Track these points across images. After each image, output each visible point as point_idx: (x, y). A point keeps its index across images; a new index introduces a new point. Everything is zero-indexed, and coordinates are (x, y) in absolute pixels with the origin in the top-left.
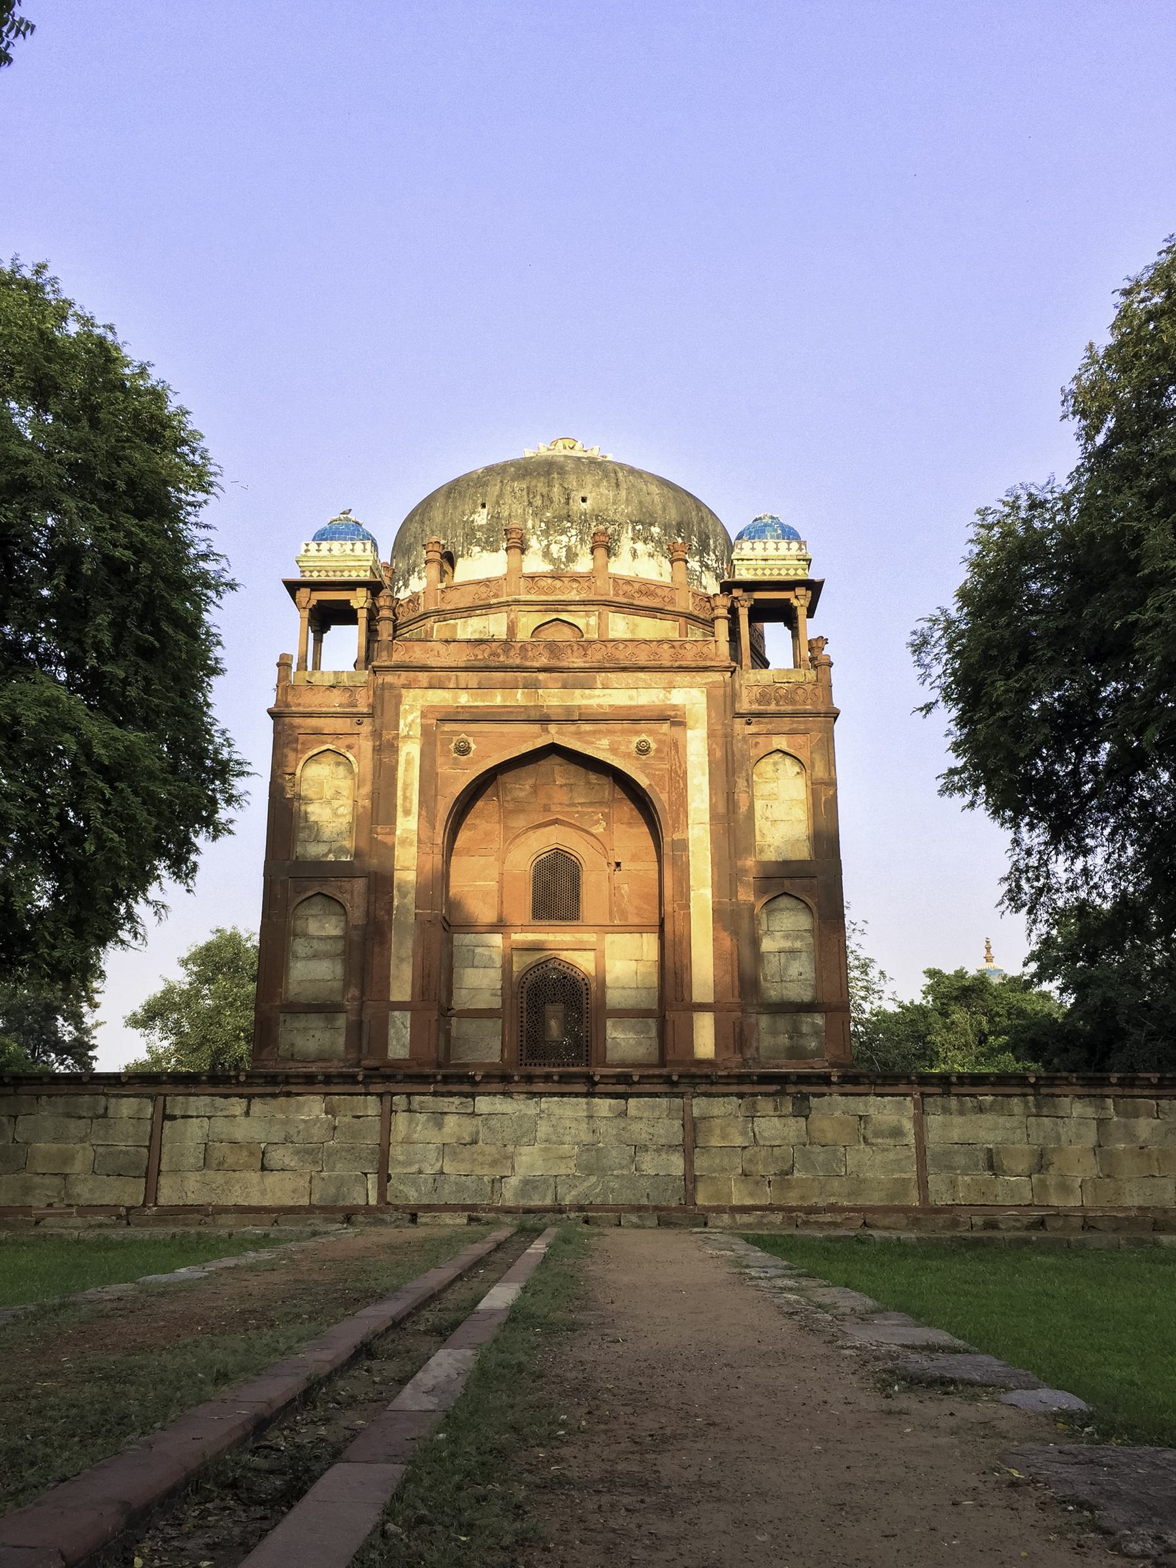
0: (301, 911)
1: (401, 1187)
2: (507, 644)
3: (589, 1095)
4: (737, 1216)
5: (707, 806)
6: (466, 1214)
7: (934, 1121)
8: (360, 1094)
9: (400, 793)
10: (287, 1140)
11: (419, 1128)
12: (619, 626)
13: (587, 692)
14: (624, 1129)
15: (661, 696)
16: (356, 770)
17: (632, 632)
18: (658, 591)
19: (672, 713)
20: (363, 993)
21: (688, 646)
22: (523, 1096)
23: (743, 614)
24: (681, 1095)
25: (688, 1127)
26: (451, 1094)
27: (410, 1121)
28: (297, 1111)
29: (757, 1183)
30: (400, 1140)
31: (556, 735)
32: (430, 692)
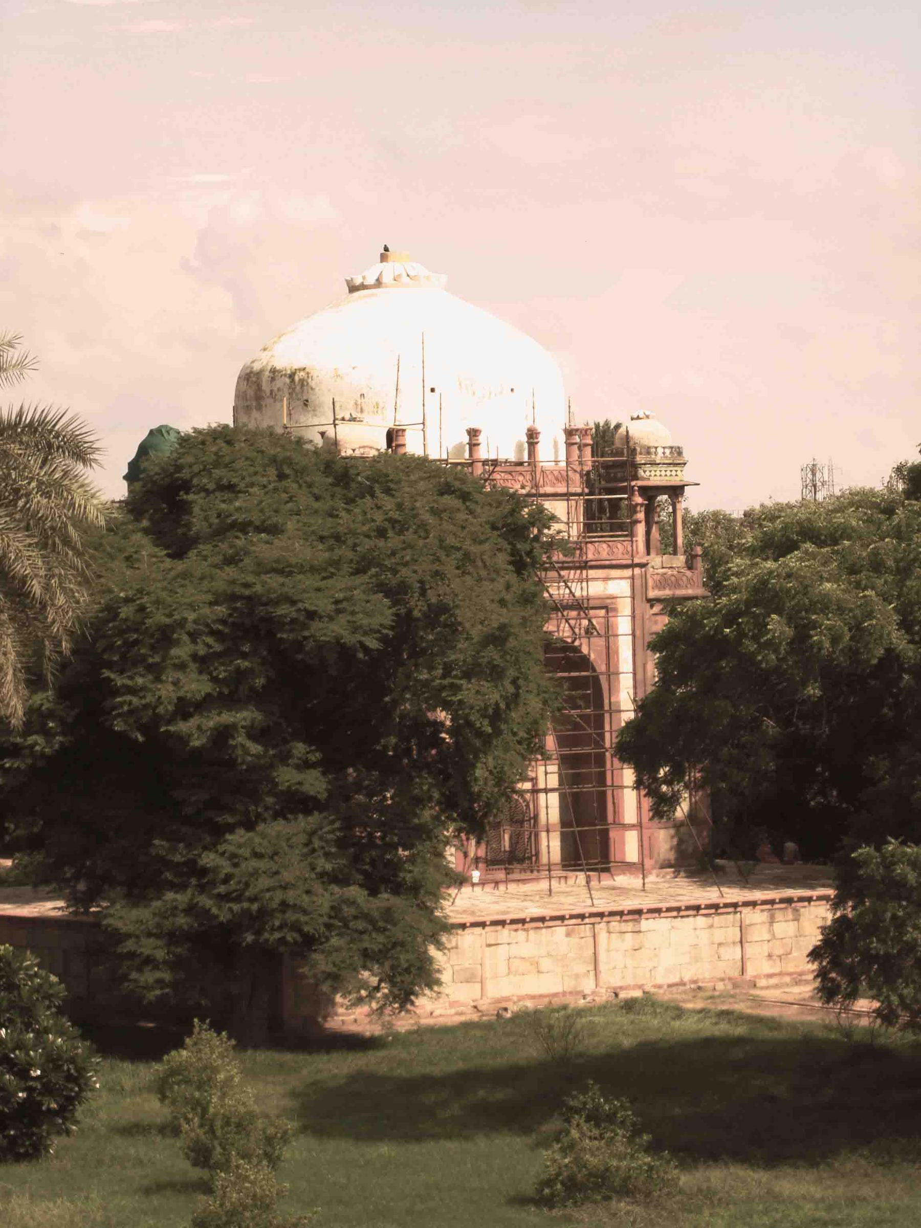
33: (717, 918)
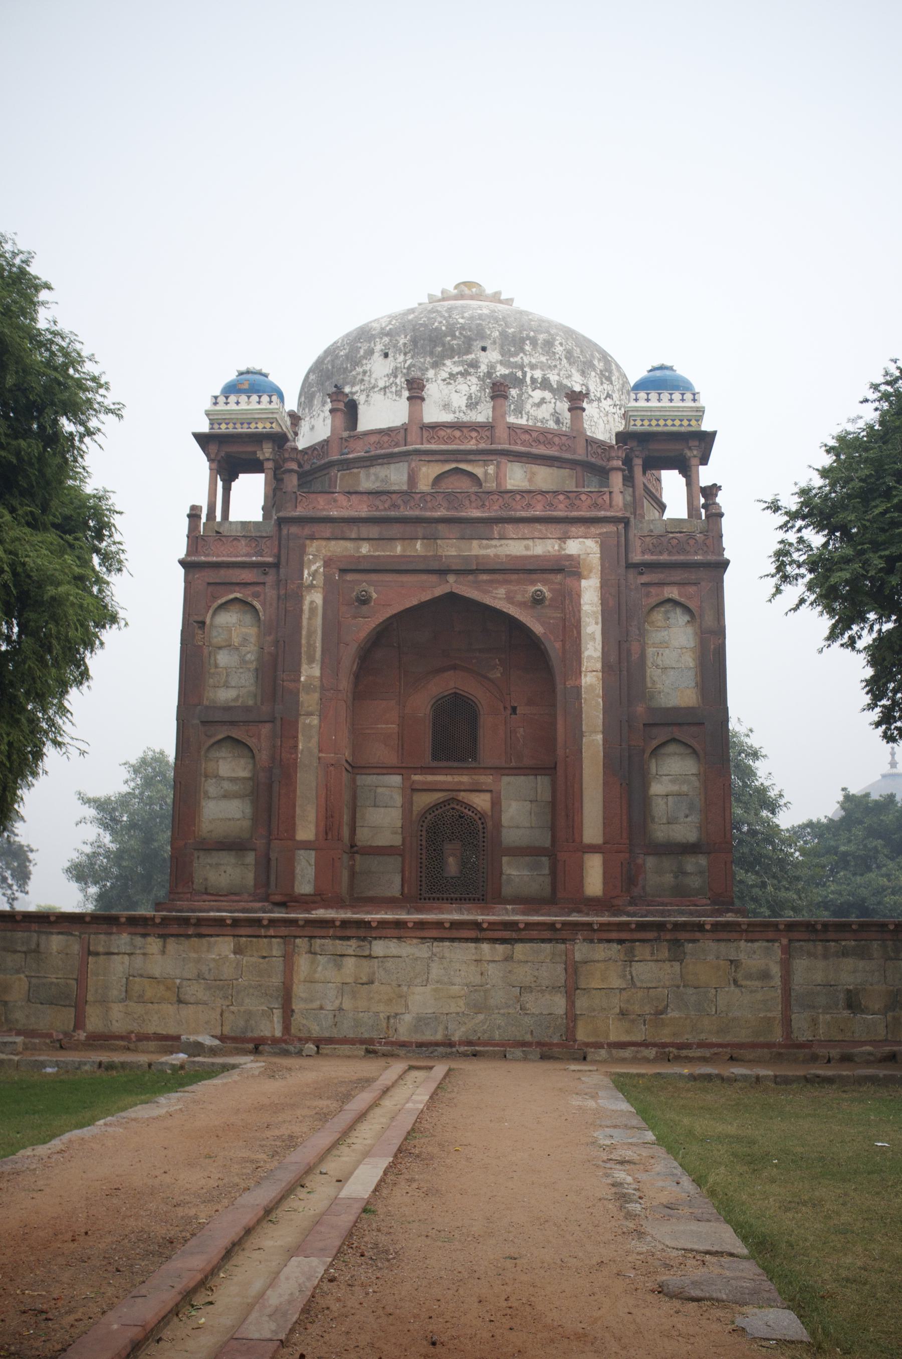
0: (214, 754)
1: (304, 1022)
2: (408, 494)
3: (476, 940)
4: (614, 1051)
5: (598, 654)
6: (364, 1047)
7: (800, 965)
8: (265, 937)
9: (304, 641)
10: (200, 976)
11: (320, 969)
12: (516, 477)
13: (485, 542)
14: (510, 972)
15: (556, 547)
16: (262, 618)
17: (530, 480)
18: (556, 440)
19: (567, 563)
20: (270, 833)
21: (583, 497)
22: (415, 941)
23: (638, 462)
24: (564, 941)
25: (570, 971)
26: (348, 938)
27: (313, 962)
28: (208, 951)
29: (633, 1021)
30: (302, 979)
31: (453, 584)
32: (333, 543)
33: (519, 947)
